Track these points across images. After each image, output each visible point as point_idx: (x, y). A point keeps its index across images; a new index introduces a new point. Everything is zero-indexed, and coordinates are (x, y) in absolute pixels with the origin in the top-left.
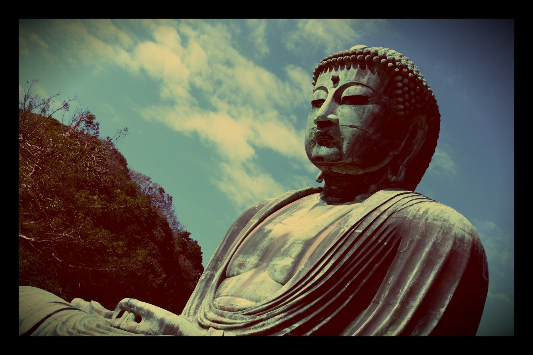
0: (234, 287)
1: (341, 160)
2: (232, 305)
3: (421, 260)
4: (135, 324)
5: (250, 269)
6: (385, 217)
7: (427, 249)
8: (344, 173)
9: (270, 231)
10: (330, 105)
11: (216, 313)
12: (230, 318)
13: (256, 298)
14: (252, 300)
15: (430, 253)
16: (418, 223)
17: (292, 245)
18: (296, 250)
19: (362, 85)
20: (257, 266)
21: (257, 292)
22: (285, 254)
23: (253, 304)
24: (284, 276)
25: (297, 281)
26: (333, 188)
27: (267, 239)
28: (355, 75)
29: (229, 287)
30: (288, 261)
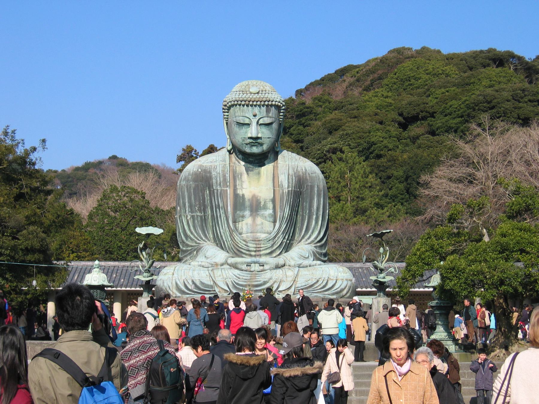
3: (316, 195)
4: (262, 268)
5: (248, 218)
6: (294, 178)
7: (316, 189)
9: (243, 195)
10: (257, 130)
11: (254, 244)
12: (264, 244)
13: (266, 231)
14: (265, 233)
15: (318, 191)
16: (306, 177)
18: (270, 205)
20: (251, 215)
22: (265, 208)
23: (267, 235)
26: (251, 159)
27: (247, 200)
29: (244, 228)
30: (271, 211)
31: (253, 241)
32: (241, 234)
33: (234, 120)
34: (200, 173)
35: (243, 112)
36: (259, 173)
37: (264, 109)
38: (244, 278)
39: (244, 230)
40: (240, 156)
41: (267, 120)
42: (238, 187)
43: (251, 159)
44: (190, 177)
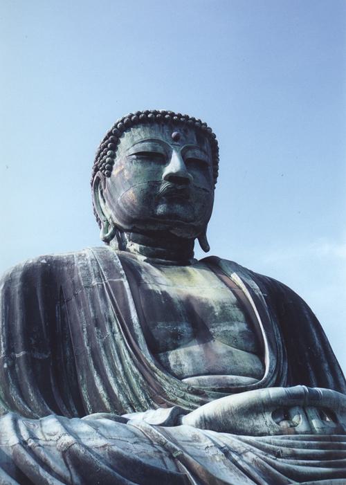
0: (194, 360)
1: (192, 221)
2: (232, 385)
8: (179, 235)
9: (165, 294)
17: (223, 307)
18: (236, 313)
19: (205, 152)
21: (241, 365)
22: (226, 317)
24: (250, 345)
25: (274, 347)
26: (160, 249)
28: (195, 140)
29: (183, 363)
31: (220, 390)
32: (180, 377)
33: (132, 151)
34: (44, 266)
35: (150, 133)
36: (184, 271)
37: (192, 134)
38: (299, 451)
39: (187, 366)
40: (136, 246)
41: (198, 154)
42: (145, 281)
43: (160, 249)
44: (19, 275)
